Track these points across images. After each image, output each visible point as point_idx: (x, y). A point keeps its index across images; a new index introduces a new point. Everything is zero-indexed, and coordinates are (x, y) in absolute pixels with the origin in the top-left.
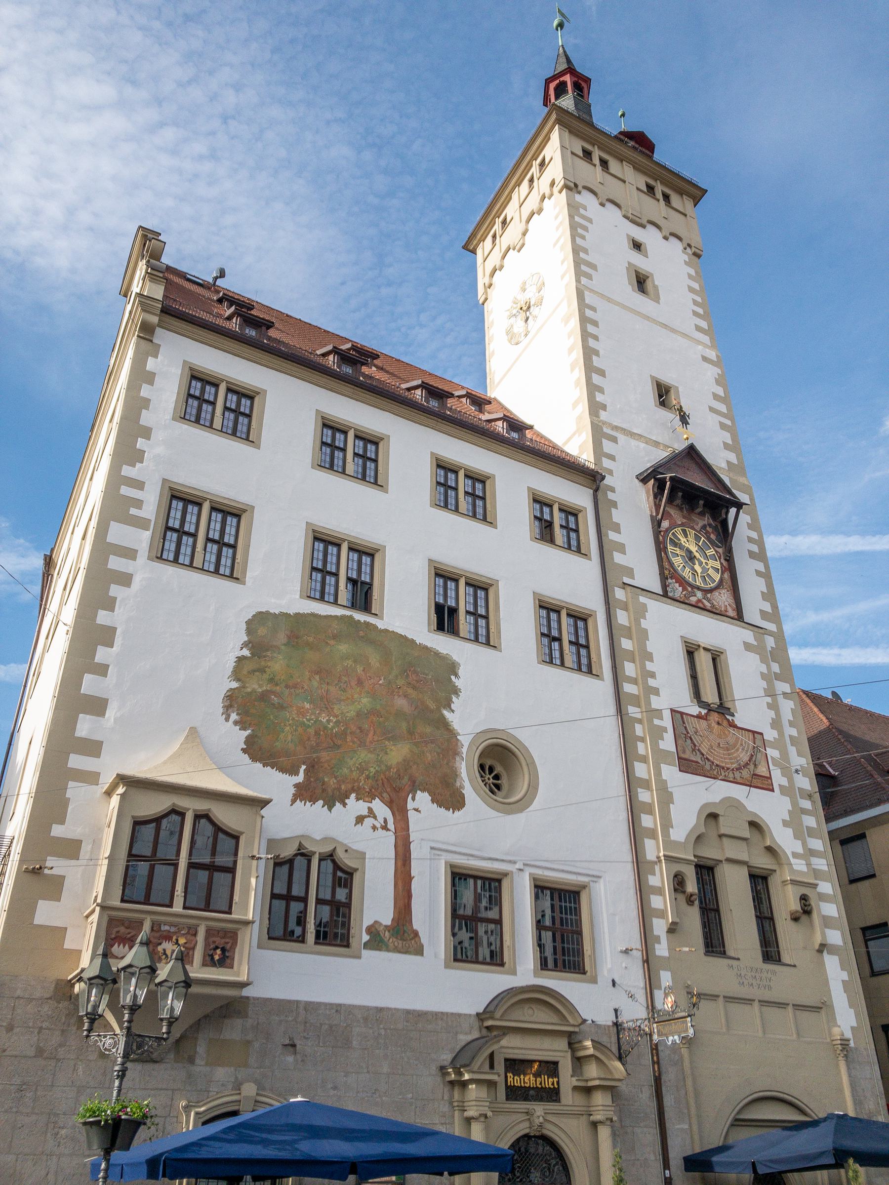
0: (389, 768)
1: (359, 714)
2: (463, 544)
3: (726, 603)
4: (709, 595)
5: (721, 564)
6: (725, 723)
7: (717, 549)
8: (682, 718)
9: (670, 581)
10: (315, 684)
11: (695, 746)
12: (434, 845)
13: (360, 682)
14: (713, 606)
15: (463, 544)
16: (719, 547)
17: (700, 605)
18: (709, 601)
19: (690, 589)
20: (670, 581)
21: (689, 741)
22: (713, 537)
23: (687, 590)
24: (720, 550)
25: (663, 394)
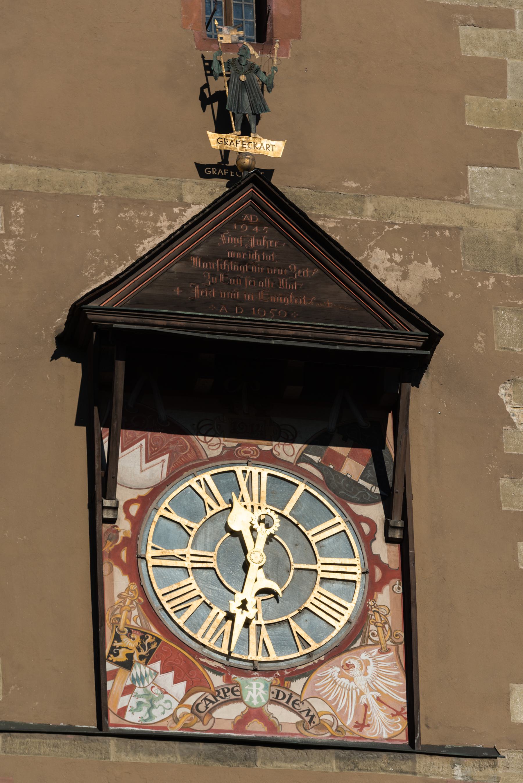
3: (369, 697)
4: (296, 686)
5: (373, 560)
9: (139, 669)
14: (310, 718)
16: (366, 499)
17: (256, 729)
18: (292, 703)
19: (218, 681)
20: (139, 669)
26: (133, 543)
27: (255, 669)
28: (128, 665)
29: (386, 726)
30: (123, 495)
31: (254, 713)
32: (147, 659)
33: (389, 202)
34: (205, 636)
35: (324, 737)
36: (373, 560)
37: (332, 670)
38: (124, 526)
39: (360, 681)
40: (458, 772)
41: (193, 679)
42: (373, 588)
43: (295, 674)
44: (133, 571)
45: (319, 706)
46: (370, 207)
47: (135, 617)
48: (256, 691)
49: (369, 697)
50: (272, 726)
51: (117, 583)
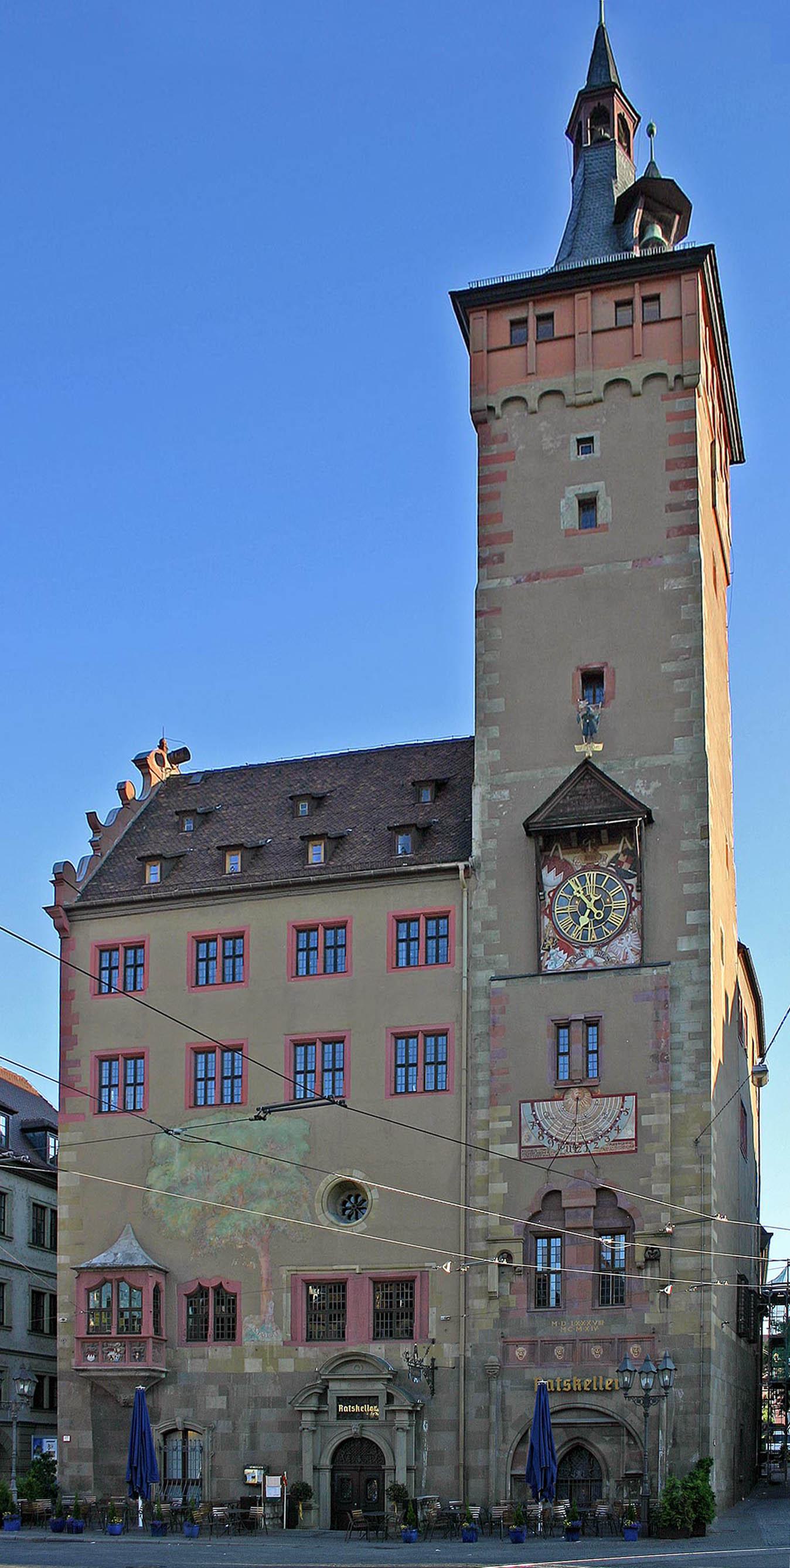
0: (254, 1221)
1: (232, 1188)
2: (321, 1005)
4: (604, 949)
5: (632, 899)
6: (588, 1095)
7: (628, 881)
8: (533, 1106)
10: (200, 1174)
11: (543, 1130)
12: (288, 1268)
13: (231, 1162)
15: (321, 1005)
19: (578, 951)
20: (552, 951)
21: (537, 1127)
22: (626, 867)
23: (573, 953)
24: (633, 881)
25: (592, 679)
26: (550, 906)
27: (591, 945)
28: (548, 950)
29: (633, 959)
30: (547, 889)
31: (591, 961)
32: (554, 947)
33: (645, 759)
34: (573, 936)
35: (612, 966)
36: (632, 899)
37: (616, 941)
38: (548, 901)
39: (626, 944)
40: (655, 972)
41: (569, 951)
42: (631, 909)
43: (604, 945)
44: (550, 917)
45: (611, 955)
46: (637, 763)
47: (551, 933)
48: (590, 953)
49: (628, 950)
50: (595, 965)
51: (546, 921)
